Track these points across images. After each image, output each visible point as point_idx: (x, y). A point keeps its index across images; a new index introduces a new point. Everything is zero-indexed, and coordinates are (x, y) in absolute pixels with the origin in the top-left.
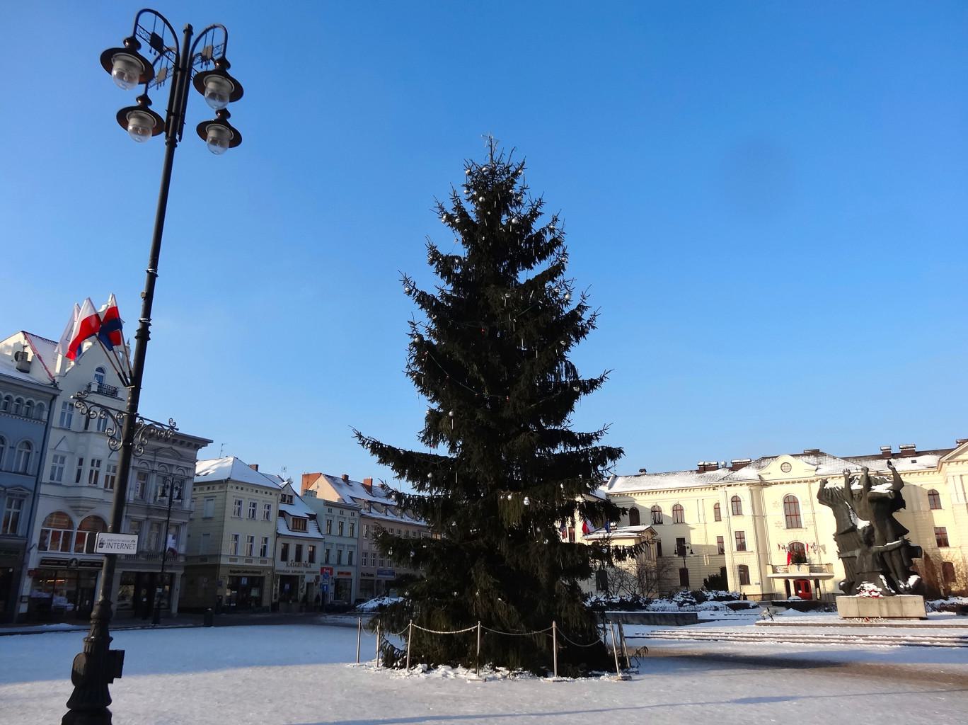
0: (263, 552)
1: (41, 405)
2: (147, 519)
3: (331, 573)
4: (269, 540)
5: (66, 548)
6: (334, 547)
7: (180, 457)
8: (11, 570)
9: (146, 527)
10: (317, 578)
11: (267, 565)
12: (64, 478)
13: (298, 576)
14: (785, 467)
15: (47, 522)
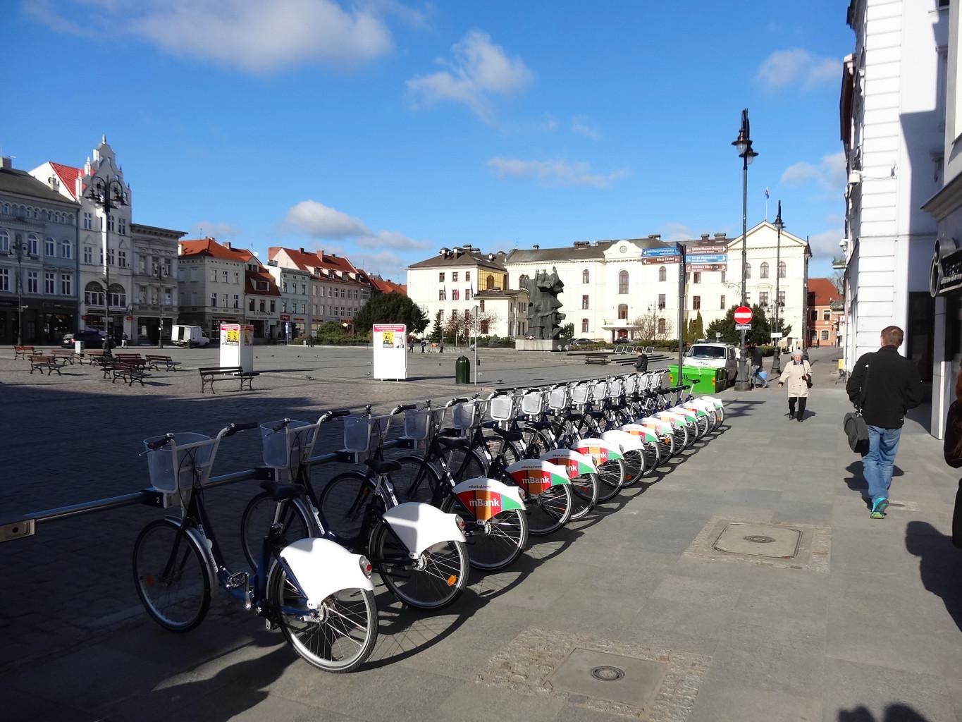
0: (236, 306)
1: (71, 216)
2: (150, 285)
3: (289, 319)
4: (239, 297)
5: (101, 303)
6: (290, 301)
7: (167, 244)
8: (71, 316)
9: (149, 291)
10: (278, 322)
11: (240, 313)
12: (93, 260)
13: (263, 321)
14: (623, 249)
15: (88, 287)
